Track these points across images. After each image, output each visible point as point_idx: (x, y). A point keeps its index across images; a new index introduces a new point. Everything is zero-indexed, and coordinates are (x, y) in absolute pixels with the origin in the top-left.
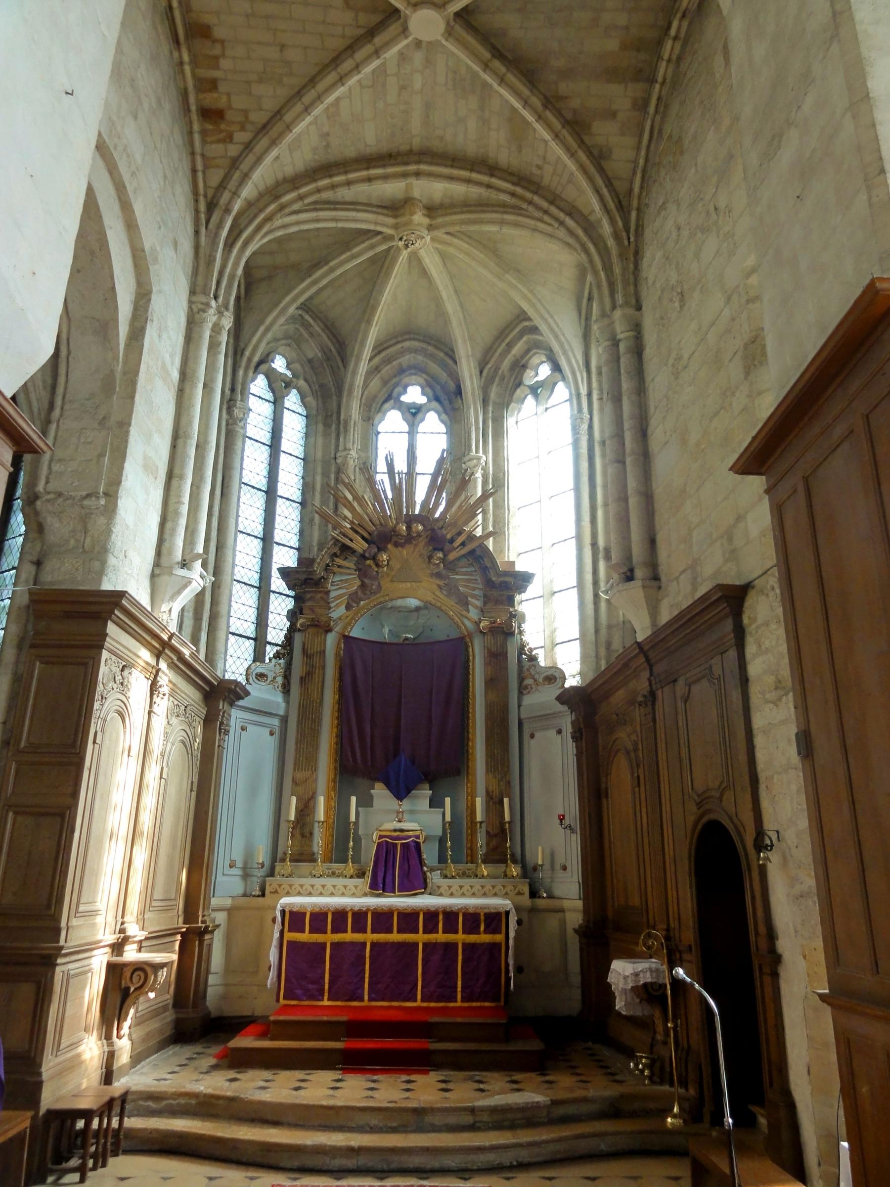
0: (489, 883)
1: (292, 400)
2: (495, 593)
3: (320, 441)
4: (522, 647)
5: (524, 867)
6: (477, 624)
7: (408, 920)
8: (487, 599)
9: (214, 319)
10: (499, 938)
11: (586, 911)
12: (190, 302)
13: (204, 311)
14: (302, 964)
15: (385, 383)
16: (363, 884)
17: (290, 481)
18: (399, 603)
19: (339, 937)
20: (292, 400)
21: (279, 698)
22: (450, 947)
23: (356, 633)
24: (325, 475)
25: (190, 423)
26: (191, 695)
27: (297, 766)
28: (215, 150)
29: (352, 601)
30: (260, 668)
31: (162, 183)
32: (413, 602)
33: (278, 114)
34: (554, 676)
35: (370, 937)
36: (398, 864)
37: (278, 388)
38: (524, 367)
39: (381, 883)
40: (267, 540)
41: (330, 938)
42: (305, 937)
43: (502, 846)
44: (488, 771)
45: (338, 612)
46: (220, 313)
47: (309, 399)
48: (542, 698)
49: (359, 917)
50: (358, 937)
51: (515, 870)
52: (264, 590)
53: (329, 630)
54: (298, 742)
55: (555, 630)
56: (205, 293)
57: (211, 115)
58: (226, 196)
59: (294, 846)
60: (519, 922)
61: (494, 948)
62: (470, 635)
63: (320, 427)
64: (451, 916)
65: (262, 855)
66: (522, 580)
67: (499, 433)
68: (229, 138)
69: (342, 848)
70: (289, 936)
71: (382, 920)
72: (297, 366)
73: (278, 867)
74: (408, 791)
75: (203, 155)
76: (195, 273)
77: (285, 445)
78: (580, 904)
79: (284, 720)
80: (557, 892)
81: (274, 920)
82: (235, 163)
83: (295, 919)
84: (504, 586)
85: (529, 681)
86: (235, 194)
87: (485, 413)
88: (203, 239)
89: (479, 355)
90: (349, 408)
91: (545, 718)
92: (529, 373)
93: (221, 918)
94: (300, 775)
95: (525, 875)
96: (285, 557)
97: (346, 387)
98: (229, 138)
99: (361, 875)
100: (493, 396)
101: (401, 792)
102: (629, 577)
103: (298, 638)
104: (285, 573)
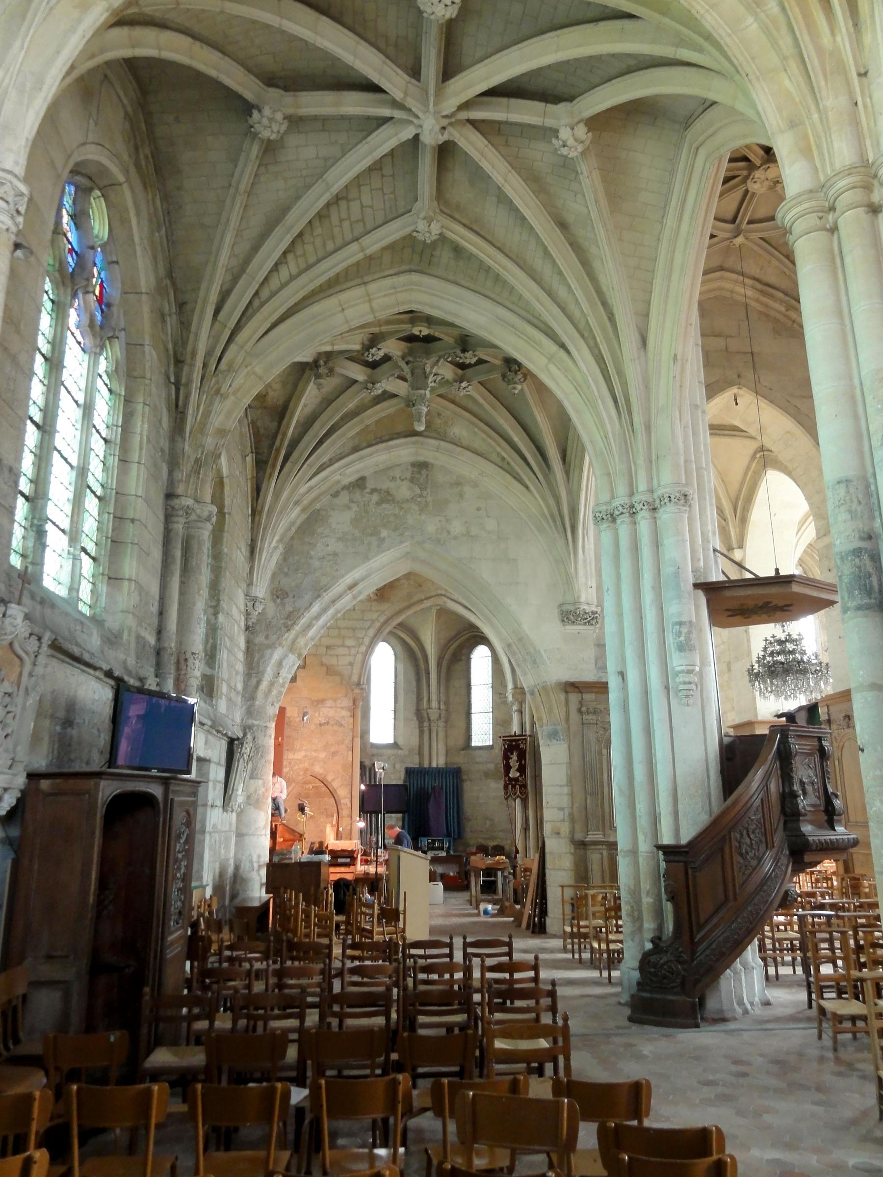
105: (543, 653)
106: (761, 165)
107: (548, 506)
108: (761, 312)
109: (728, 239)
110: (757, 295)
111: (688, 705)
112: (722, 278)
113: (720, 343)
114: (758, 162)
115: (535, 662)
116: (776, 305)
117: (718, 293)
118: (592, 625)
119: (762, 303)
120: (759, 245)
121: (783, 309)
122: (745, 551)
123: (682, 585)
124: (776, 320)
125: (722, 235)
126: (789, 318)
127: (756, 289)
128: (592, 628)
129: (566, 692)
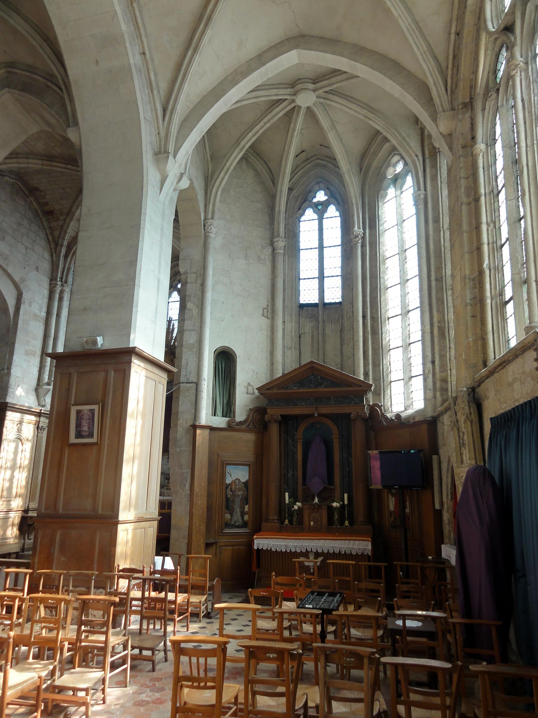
9: (60, 289)
12: (50, 284)
13: (55, 287)
25: (50, 331)
28: (54, 224)
31: (24, 252)
33: (71, 209)
46: (62, 285)
56: (56, 280)
57: (49, 213)
58: (60, 240)
68: (58, 219)
75: (50, 227)
76: (52, 272)
82: (62, 227)
86: (64, 239)
88: (54, 258)
98: (58, 219)
122: (79, 128)
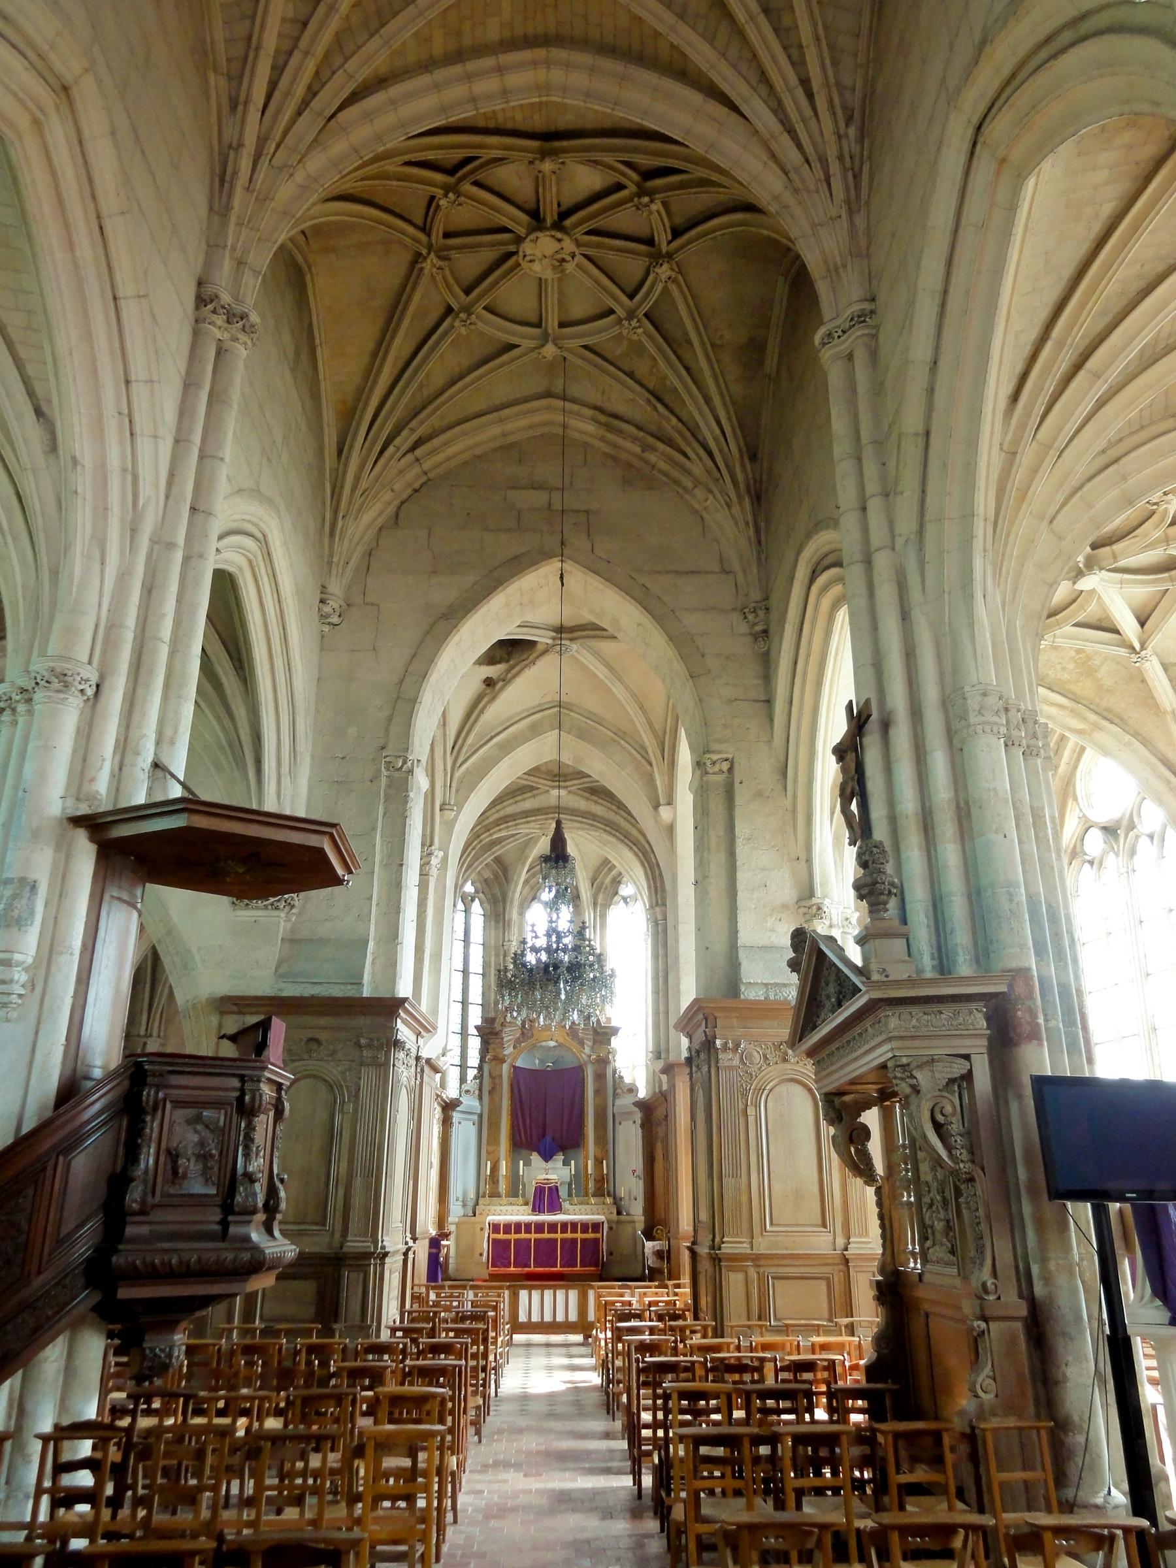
0: (594, 1208)
1: (476, 907)
2: (599, 1038)
3: (493, 934)
4: (614, 1072)
5: (615, 1198)
6: (590, 1056)
7: (553, 1227)
8: (595, 1042)
10: (599, 1235)
11: (646, 1221)
14: (500, 1250)
15: (532, 888)
16: (529, 1208)
17: (476, 965)
18: (544, 1044)
19: (518, 1236)
20: (476, 907)
21: (476, 1103)
22: (574, 1241)
23: (519, 1064)
24: (497, 956)
26: (439, 1109)
27: (489, 1143)
29: (517, 1042)
30: (465, 1087)
32: (552, 1044)
34: (632, 1090)
35: (533, 1236)
36: (546, 1198)
37: (467, 900)
38: (619, 882)
39: (537, 1208)
40: (465, 1003)
41: (513, 1237)
42: (501, 1236)
43: (603, 1187)
44: (596, 1143)
45: (509, 1050)
47: (486, 905)
48: (625, 1102)
49: (528, 1227)
50: (528, 1236)
51: (609, 1200)
52: (464, 1034)
53: (503, 1061)
54: (489, 1129)
55: (633, 1062)
59: (488, 1188)
60: (610, 1228)
61: (596, 1241)
62: (586, 1064)
63: (493, 923)
64: (574, 1225)
65: (472, 1195)
66: (615, 1031)
67: (603, 925)
69: (514, 1192)
70: (493, 1236)
71: (540, 1227)
72: (478, 885)
73: (481, 1201)
74: (551, 1157)
77: (472, 939)
78: (643, 1218)
79: (481, 1116)
80: (632, 1212)
81: (482, 1229)
83: (495, 1228)
84: (603, 1035)
85: (619, 1091)
87: (595, 912)
89: (591, 875)
90: (510, 912)
91: (627, 1115)
92: (622, 886)
93: (452, 1228)
94: (491, 1148)
95: (615, 1203)
96: (475, 1017)
97: (509, 900)
99: (526, 1204)
100: (600, 900)
101: (547, 1157)
102: (659, 1057)
103: (486, 1067)
104: (477, 1027)
105: (194, 950)
106: (527, 236)
107: (224, 729)
108: (606, 455)
109: (535, 348)
110: (602, 432)
111: (8, 1020)
112: (548, 408)
113: (540, 498)
114: (522, 231)
115: (185, 966)
116: (627, 444)
117: (546, 429)
118: (277, 908)
119: (609, 443)
120: (584, 359)
121: (638, 450)
122: (675, 809)
123: (24, 817)
124: (630, 466)
125: (527, 344)
126: (647, 462)
127: (600, 423)
128: (276, 913)
129: (222, 1013)
